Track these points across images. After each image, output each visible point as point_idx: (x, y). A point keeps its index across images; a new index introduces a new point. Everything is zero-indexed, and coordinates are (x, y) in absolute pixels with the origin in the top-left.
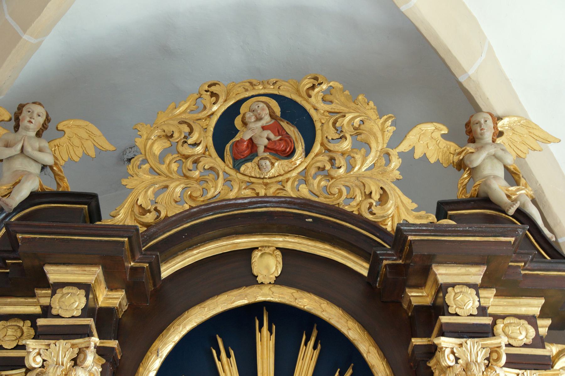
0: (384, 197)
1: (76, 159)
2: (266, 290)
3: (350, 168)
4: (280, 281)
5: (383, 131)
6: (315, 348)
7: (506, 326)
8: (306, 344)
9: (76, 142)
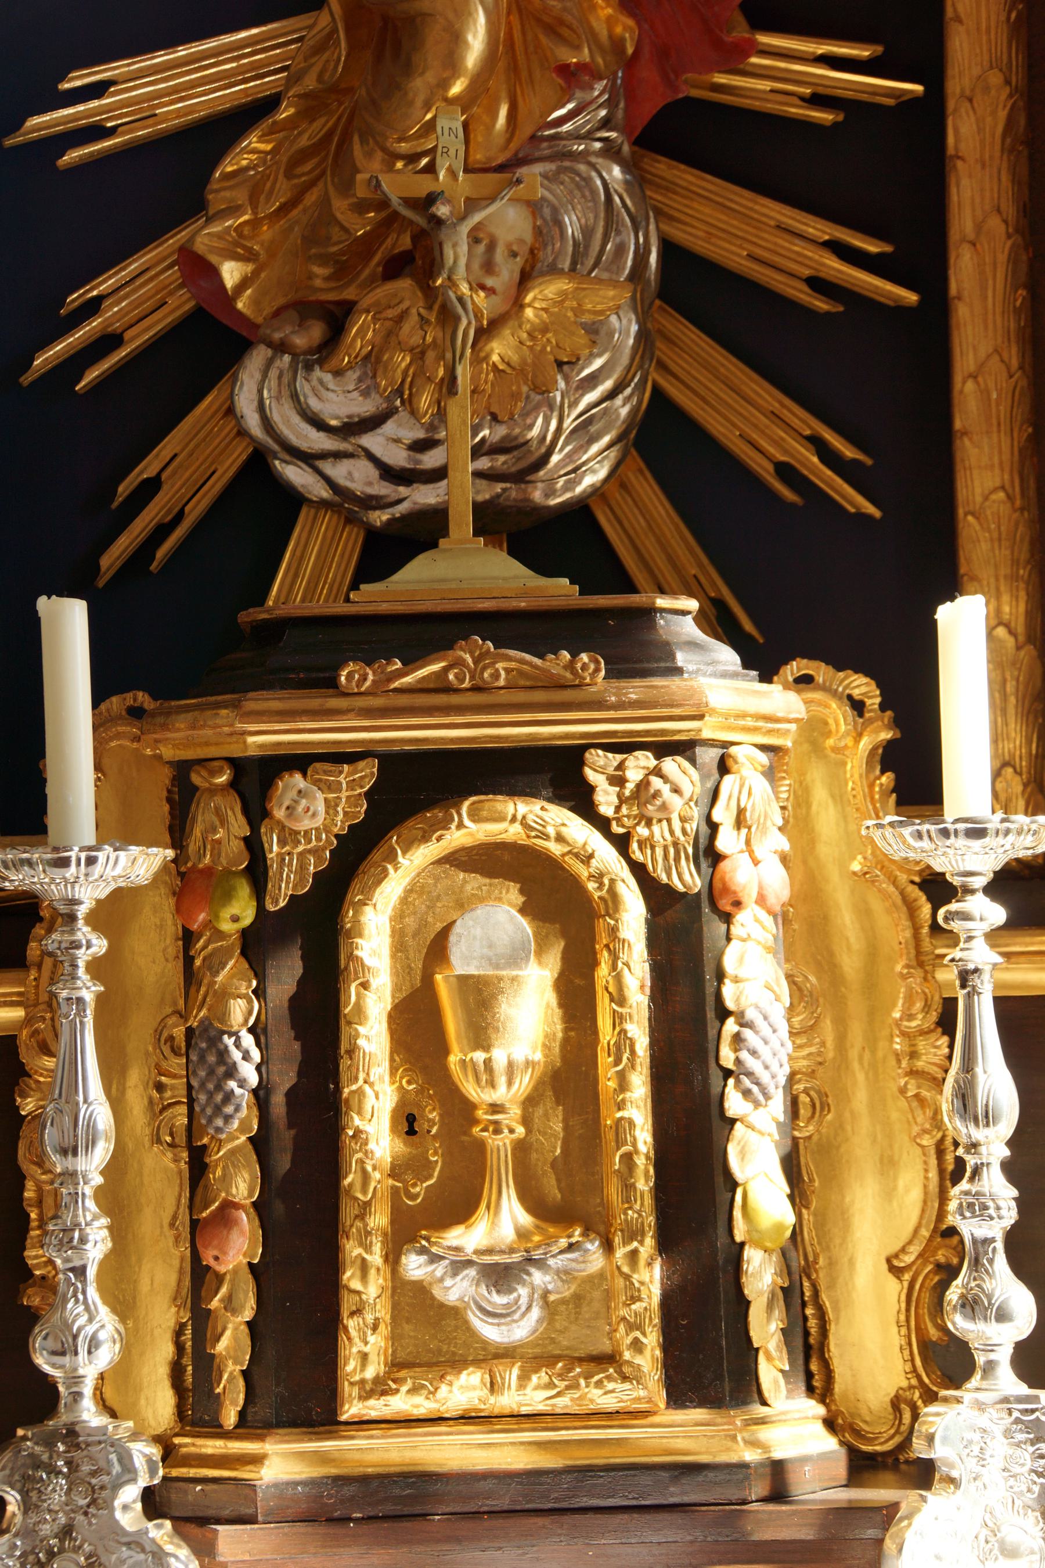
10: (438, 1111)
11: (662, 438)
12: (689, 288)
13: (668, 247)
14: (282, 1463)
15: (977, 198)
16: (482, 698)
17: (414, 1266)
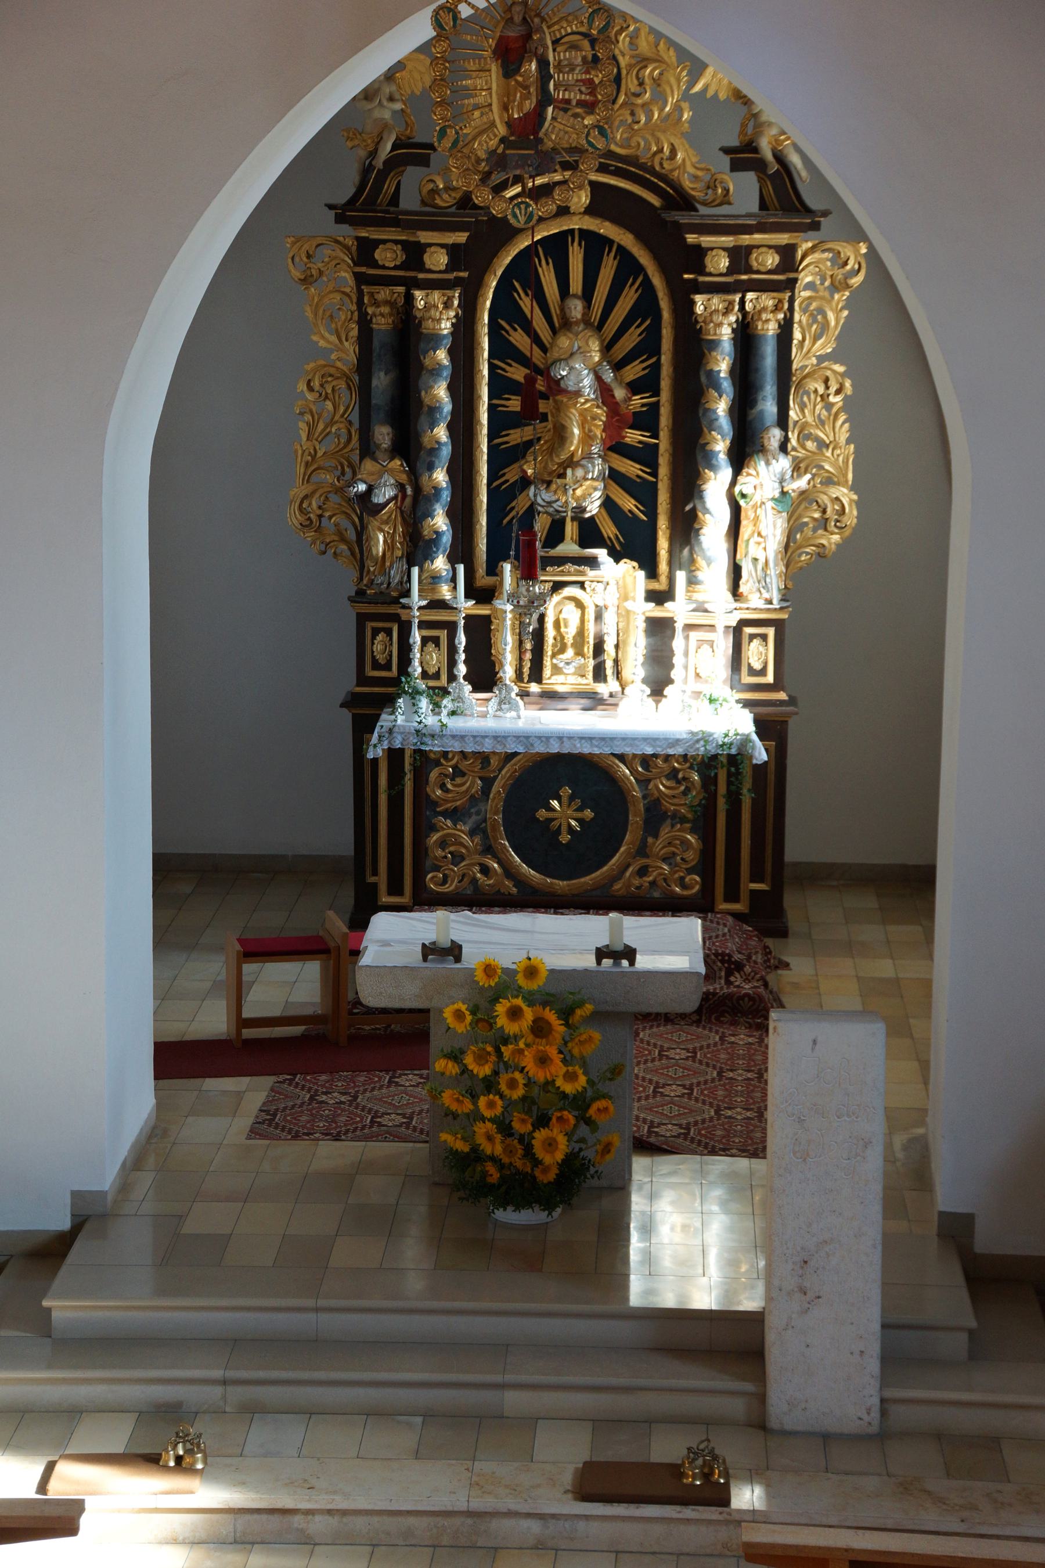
0: (673, 152)
1: (418, 93)
2: (576, 218)
3: (649, 116)
4: (590, 211)
5: (679, 81)
6: (615, 258)
7: (759, 254)
8: (608, 255)
9: (417, 76)
10: (560, 638)
11: (608, 504)
12: (615, 476)
13: (610, 468)
14: (534, 688)
15: (664, 471)
16: (569, 574)
17: (555, 661)
